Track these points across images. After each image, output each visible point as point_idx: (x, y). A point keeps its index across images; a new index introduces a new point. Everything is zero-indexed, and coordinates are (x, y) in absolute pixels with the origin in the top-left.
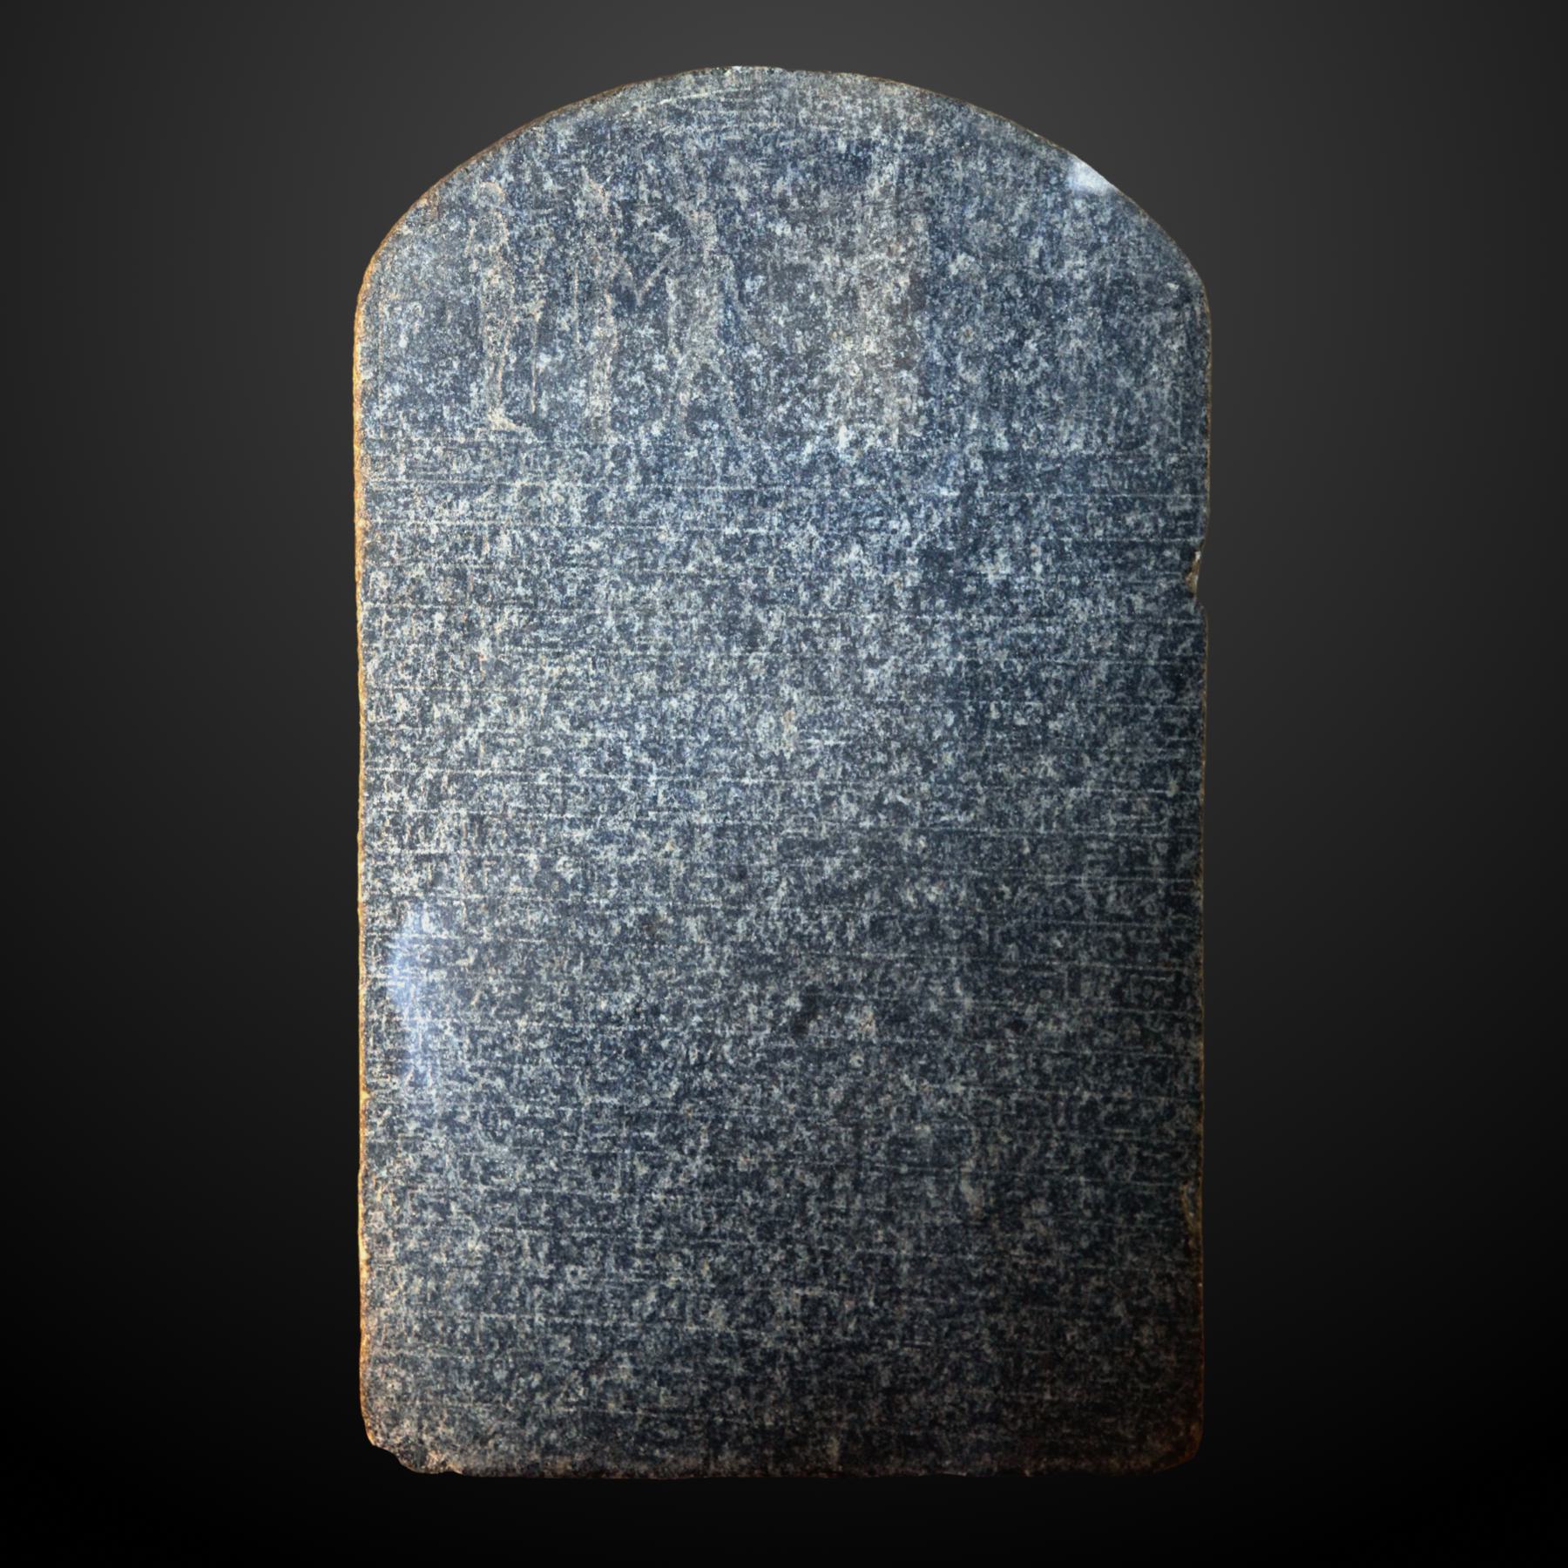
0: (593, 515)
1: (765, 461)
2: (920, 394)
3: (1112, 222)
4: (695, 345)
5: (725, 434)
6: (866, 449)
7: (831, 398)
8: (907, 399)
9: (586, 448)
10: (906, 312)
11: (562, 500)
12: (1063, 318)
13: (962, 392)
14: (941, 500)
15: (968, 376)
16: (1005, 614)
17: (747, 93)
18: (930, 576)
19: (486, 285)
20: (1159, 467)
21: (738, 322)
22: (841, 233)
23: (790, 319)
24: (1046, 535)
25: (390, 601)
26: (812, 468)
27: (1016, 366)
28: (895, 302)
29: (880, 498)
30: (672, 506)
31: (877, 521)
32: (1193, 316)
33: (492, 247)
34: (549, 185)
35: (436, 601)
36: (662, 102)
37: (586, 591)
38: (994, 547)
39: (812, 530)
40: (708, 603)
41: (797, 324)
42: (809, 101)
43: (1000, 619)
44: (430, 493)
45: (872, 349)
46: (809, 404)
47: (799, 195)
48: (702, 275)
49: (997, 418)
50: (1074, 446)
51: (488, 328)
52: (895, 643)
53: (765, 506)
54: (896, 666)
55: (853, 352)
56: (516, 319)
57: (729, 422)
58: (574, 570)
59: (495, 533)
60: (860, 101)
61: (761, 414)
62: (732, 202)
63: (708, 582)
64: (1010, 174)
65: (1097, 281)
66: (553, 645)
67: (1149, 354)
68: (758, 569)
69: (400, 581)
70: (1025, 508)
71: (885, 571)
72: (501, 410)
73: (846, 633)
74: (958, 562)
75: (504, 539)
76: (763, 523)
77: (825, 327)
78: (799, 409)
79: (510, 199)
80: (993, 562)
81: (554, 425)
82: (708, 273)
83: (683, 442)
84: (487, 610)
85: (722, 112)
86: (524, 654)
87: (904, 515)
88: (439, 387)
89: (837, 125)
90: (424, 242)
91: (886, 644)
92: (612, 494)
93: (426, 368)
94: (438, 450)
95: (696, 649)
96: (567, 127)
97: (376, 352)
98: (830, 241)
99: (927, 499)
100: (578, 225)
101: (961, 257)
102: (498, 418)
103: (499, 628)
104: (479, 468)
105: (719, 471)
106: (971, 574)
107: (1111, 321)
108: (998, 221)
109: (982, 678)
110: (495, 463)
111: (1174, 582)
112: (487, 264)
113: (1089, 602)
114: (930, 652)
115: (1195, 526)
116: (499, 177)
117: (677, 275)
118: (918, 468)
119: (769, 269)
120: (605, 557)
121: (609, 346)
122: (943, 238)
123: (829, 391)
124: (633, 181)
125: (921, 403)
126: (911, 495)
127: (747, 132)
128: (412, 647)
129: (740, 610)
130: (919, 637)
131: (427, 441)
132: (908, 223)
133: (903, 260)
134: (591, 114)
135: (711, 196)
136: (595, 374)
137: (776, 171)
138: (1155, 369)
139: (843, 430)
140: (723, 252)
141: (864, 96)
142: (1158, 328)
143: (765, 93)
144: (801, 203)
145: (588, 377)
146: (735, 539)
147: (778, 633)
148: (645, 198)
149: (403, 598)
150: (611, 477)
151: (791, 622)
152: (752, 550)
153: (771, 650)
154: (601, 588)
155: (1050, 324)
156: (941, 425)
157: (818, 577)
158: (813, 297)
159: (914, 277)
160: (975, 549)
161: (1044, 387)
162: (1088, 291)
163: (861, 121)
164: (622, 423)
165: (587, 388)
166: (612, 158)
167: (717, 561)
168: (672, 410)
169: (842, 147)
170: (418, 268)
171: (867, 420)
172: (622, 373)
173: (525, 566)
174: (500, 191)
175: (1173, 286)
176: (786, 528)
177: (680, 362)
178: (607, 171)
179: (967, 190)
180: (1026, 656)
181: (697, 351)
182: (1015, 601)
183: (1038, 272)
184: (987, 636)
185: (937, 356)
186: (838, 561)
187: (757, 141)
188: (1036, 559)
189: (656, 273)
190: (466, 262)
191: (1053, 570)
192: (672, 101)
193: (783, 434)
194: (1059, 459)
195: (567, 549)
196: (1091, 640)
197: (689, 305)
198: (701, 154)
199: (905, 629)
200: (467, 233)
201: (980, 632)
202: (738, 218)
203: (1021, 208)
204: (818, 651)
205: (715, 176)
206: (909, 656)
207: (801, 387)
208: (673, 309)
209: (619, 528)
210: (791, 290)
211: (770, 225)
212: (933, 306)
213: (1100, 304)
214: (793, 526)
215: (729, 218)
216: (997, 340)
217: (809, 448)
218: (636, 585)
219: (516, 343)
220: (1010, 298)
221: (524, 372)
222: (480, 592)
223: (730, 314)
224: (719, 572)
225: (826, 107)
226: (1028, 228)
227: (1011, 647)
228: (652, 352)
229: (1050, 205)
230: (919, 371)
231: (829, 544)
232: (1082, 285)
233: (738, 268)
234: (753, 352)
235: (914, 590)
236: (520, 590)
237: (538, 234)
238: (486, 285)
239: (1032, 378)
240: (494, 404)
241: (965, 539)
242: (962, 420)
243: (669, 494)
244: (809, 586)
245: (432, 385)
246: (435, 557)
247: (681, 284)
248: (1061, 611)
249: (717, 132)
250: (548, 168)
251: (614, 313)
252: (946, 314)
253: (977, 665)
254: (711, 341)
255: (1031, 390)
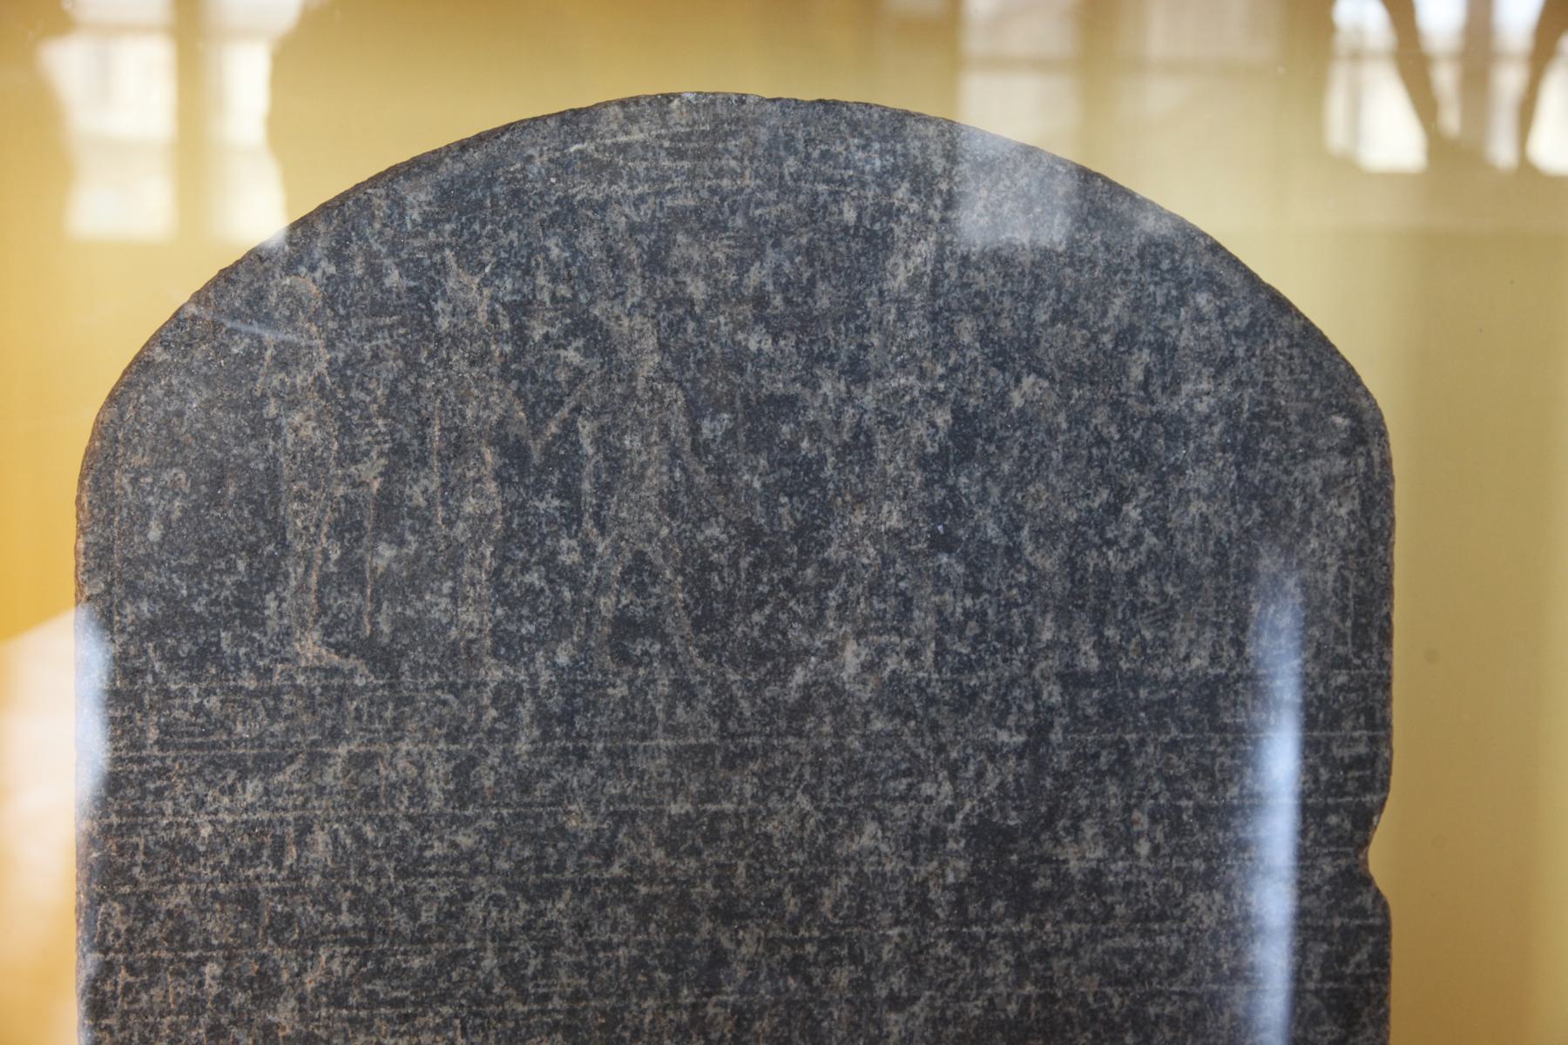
0: (463, 790)
1: (732, 698)
2: (966, 589)
3: (1251, 326)
4: (623, 523)
5: (671, 658)
6: (886, 674)
7: (833, 598)
8: (948, 597)
9: (453, 688)
10: (946, 465)
11: (413, 772)
12: (1179, 470)
13: (1030, 585)
14: (997, 749)
15: (1038, 559)
16: (1095, 921)
17: (704, 134)
18: (983, 865)
19: (291, 438)
20: (1321, 691)
21: (690, 486)
22: (847, 347)
23: (771, 480)
24: (1155, 797)
25: (131, 949)
26: (804, 707)
27: (1110, 543)
28: (930, 450)
29: (907, 748)
30: (588, 773)
31: (903, 784)
32: (1370, 465)
33: (301, 378)
34: (393, 278)
35: (207, 945)
36: (572, 149)
37: (452, 913)
38: (1078, 818)
39: (804, 802)
40: (644, 922)
41: (782, 487)
42: (800, 146)
43: (1087, 928)
44: (199, 772)
45: (895, 521)
46: (799, 609)
47: (785, 289)
48: (635, 413)
49: (1083, 623)
50: (1196, 662)
51: (295, 506)
52: (931, 972)
53: (732, 767)
54: (932, 1008)
55: (866, 527)
56: (340, 491)
57: (676, 640)
58: (432, 882)
59: (305, 829)
60: (876, 146)
61: (726, 626)
62: (680, 302)
63: (643, 890)
64: (1101, 255)
65: (1229, 414)
66: (397, 1003)
67: (1305, 522)
68: (719, 866)
69: (148, 915)
70: (1123, 765)
71: (915, 861)
72: (316, 635)
73: (855, 959)
74: (1024, 843)
75: (321, 837)
76: (728, 795)
77: (824, 490)
78: (784, 617)
79: (330, 301)
80: (1077, 841)
81: (402, 654)
82: (644, 411)
83: (605, 674)
84: (292, 953)
85: (666, 163)
86: (351, 1021)
87: (943, 774)
88: (215, 602)
89: (843, 182)
90: (189, 372)
91: (917, 974)
92: (494, 760)
93: (193, 572)
94: (213, 703)
95: (625, 995)
96: (421, 188)
97: (110, 549)
98: (832, 359)
99: (979, 747)
100: (439, 341)
101: (1028, 381)
102: (310, 647)
103: (310, 981)
104: (278, 727)
105: (661, 716)
106: (1045, 860)
107: (1250, 473)
108: (1083, 325)
109: (1061, 1019)
110: (305, 718)
111: (1343, 862)
112: (294, 405)
113: (1218, 896)
114: (984, 983)
115: (1373, 777)
116: (313, 268)
117: (596, 414)
118: (965, 700)
119: (738, 403)
120: (482, 858)
121: (489, 528)
122: (1002, 352)
123: (830, 587)
124: (527, 272)
125: (968, 602)
126: (954, 743)
127: (705, 194)
128: (167, 1020)
129: (694, 931)
130: (967, 960)
131: (194, 689)
132: (949, 330)
133: (941, 386)
134: (460, 167)
135: (650, 291)
136: (466, 572)
137: (748, 253)
138: (1314, 544)
139: (851, 647)
140: (667, 378)
141: (884, 139)
142: (1317, 481)
143: (734, 134)
144: (788, 301)
145: (456, 578)
146: (686, 821)
147: (752, 964)
148: (545, 297)
149: (152, 943)
150: (491, 732)
151: (772, 945)
152: (712, 837)
153: (742, 992)
154: (475, 909)
155: (1161, 480)
156: (999, 636)
157: (814, 875)
158: (805, 444)
159: (959, 412)
160: (1050, 820)
161: (1151, 575)
162: (1216, 430)
163: (879, 176)
164: (509, 647)
165: (453, 596)
166: (493, 236)
167: (659, 855)
168: (589, 625)
169: (850, 216)
170: (180, 414)
171: (888, 631)
172: (509, 569)
173: (353, 881)
174: (314, 289)
175: (1339, 420)
176: (764, 800)
177: (600, 550)
178: (486, 257)
179: (1037, 279)
180: (1127, 983)
181: (628, 531)
182: (1109, 899)
183: (1142, 401)
184: (1068, 953)
185: (992, 531)
186: (843, 848)
187: (719, 208)
188: (1140, 835)
189: (564, 412)
190: (259, 402)
191: (1166, 850)
192: (588, 146)
193: (760, 656)
194: (1174, 681)
195: (422, 849)
196: (1222, 954)
197: (615, 462)
198: (633, 229)
199: (945, 949)
200: (261, 356)
201: (1058, 949)
202: (691, 326)
203: (1116, 307)
204: (813, 990)
205: (655, 262)
206: (951, 990)
207: (788, 583)
208: (589, 467)
209: (505, 812)
210: (771, 435)
211: (740, 336)
212: (987, 455)
213: (1233, 447)
214: (775, 797)
215: (676, 327)
216: (1083, 504)
217: (799, 676)
218: (530, 900)
219: (339, 529)
220: (1101, 441)
221: (352, 571)
222: (280, 927)
223: (678, 474)
224: (661, 873)
225: (825, 155)
226: (1127, 337)
227: (1103, 970)
228: (556, 536)
229: (1160, 300)
230: (966, 554)
231: (830, 822)
232: (1207, 420)
233: (690, 403)
234: (714, 531)
235: (958, 888)
236: (345, 919)
237: (375, 356)
238: (291, 438)
239: (1133, 562)
240: (303, 625)
241: (1035, 808)
242: (1030, 626)
243: (582, 755)
244: (800, 889)
245: (203, 600)
246: (207, 873)
247: (601, 429)
248: (1177, 912)
249: (657, 194)
250: (391, 253)
251: (498, 476)
252: (1006, 467)
253: (1053, 999)
254: (649, 515)
255: (1132, 579)
